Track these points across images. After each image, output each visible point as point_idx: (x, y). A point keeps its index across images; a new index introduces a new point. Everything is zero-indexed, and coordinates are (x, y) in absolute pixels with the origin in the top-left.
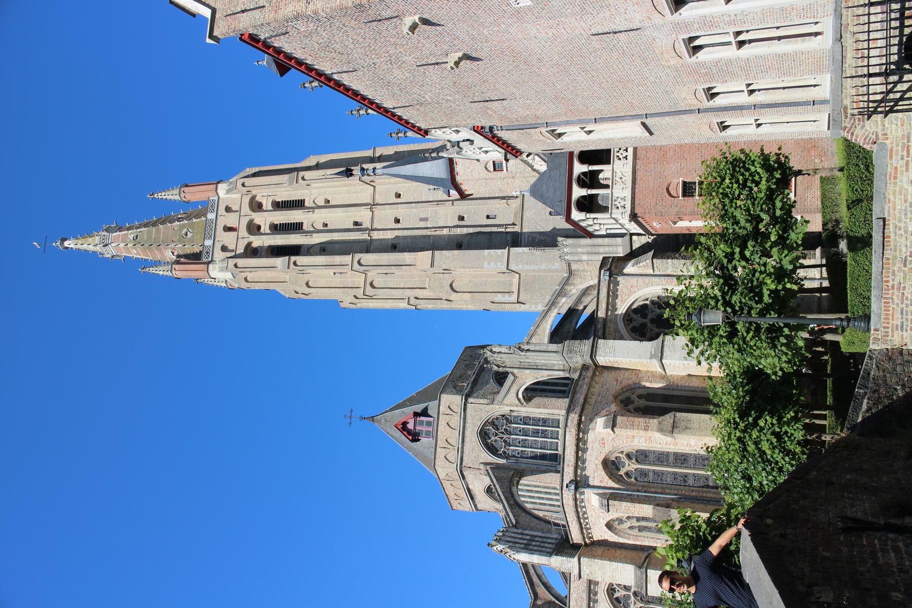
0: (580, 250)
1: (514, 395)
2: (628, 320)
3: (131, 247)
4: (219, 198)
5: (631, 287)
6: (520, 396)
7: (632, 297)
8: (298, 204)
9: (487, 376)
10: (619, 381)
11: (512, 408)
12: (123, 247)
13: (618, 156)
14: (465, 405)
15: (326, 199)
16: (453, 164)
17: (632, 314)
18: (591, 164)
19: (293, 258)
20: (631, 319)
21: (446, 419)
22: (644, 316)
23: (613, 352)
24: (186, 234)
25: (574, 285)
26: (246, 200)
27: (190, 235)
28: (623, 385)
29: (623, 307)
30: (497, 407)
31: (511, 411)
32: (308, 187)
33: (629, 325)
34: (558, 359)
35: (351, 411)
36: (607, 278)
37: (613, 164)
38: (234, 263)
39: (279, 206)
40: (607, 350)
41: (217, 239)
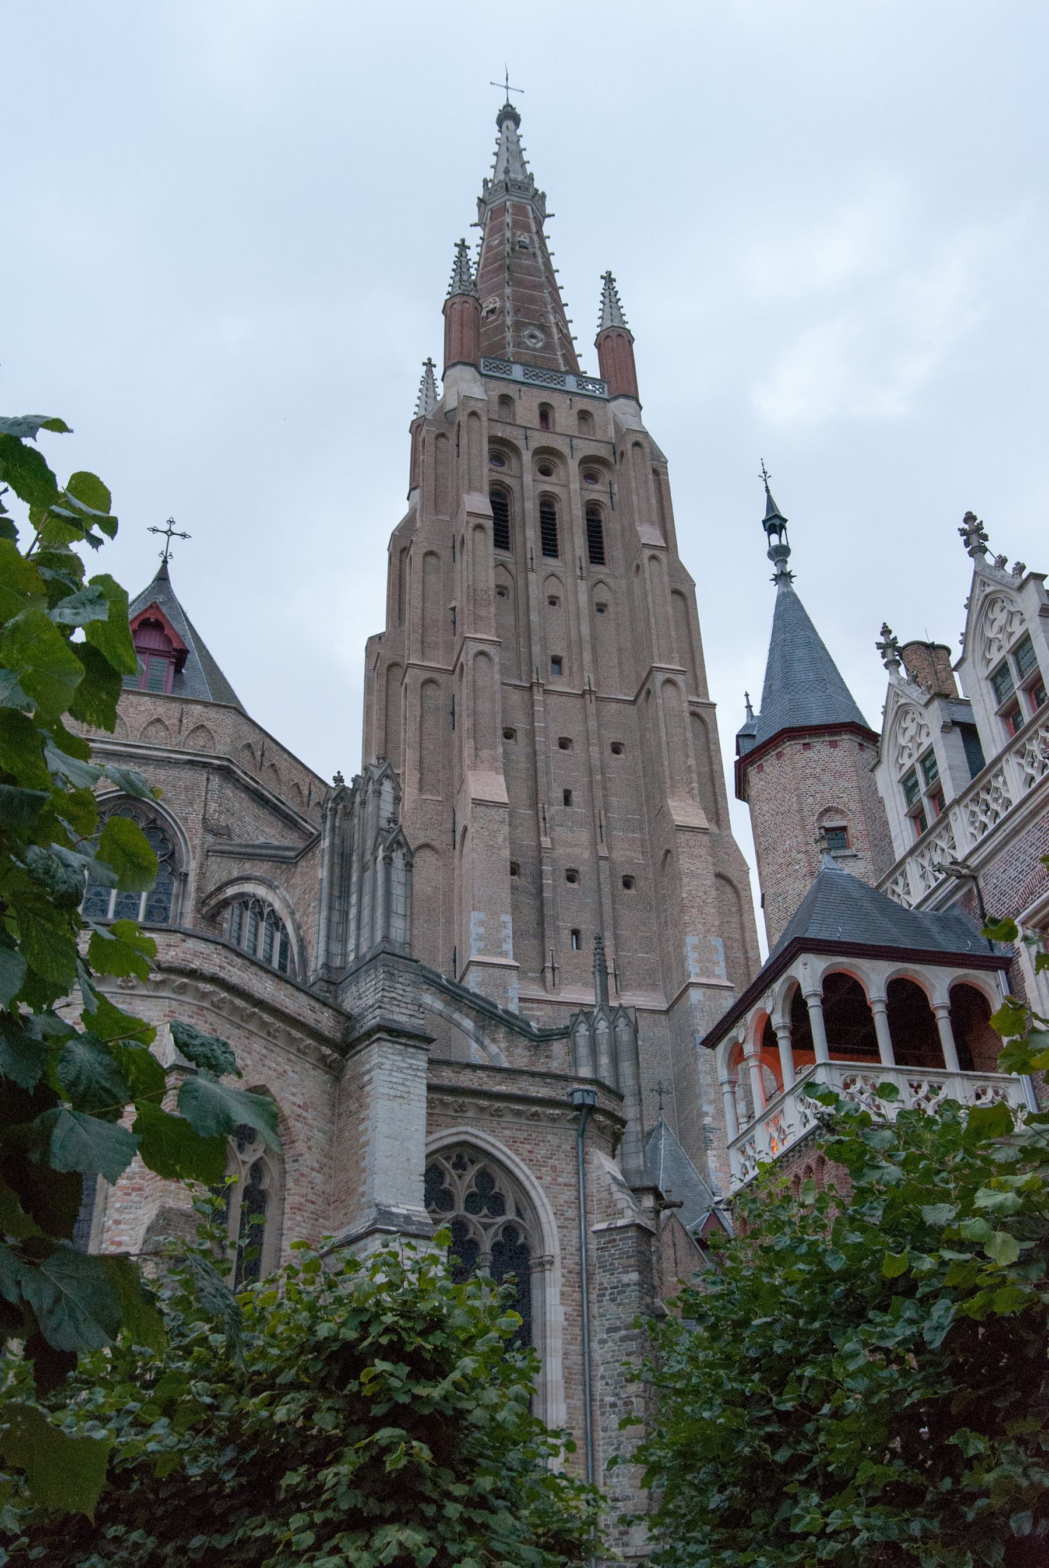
0: (604, 1060)
1: (235, 874)
2: (460, 1157)
3: (503, 235)
4: (608, 400)
5: (554, 1168)
6: (230, 891)
7: (522, 1164)
8: (596, 553)
9: (273, 832)
10: (304, 1114)
11: (192, 878)
12: (503, 221)
13: (984, 1092)
14: (205, 765)
15: (606, 605)
16: (831, 734)
17: (478, 1167)
18: (954, 1013)
19: (489, 524)
20: (464, 1169)
21: (169, 718)
22: (473, 1203)
23: (392, 1092)
24: (532, 336)
25: (508, 1049)
26: (603, 452)
27: (530, 343)
28: (291, 1122)
29: (499, 1144)
30: (197, 841)
31: (186, 875)
32: (634, 568)
33: (447, 1159)
34: (364, 949)
35: (184, 536)
36: (578, 1099)
37: (962, 1076)
39: (593, 515)
40: (398, 1077)
41: (524, 389)
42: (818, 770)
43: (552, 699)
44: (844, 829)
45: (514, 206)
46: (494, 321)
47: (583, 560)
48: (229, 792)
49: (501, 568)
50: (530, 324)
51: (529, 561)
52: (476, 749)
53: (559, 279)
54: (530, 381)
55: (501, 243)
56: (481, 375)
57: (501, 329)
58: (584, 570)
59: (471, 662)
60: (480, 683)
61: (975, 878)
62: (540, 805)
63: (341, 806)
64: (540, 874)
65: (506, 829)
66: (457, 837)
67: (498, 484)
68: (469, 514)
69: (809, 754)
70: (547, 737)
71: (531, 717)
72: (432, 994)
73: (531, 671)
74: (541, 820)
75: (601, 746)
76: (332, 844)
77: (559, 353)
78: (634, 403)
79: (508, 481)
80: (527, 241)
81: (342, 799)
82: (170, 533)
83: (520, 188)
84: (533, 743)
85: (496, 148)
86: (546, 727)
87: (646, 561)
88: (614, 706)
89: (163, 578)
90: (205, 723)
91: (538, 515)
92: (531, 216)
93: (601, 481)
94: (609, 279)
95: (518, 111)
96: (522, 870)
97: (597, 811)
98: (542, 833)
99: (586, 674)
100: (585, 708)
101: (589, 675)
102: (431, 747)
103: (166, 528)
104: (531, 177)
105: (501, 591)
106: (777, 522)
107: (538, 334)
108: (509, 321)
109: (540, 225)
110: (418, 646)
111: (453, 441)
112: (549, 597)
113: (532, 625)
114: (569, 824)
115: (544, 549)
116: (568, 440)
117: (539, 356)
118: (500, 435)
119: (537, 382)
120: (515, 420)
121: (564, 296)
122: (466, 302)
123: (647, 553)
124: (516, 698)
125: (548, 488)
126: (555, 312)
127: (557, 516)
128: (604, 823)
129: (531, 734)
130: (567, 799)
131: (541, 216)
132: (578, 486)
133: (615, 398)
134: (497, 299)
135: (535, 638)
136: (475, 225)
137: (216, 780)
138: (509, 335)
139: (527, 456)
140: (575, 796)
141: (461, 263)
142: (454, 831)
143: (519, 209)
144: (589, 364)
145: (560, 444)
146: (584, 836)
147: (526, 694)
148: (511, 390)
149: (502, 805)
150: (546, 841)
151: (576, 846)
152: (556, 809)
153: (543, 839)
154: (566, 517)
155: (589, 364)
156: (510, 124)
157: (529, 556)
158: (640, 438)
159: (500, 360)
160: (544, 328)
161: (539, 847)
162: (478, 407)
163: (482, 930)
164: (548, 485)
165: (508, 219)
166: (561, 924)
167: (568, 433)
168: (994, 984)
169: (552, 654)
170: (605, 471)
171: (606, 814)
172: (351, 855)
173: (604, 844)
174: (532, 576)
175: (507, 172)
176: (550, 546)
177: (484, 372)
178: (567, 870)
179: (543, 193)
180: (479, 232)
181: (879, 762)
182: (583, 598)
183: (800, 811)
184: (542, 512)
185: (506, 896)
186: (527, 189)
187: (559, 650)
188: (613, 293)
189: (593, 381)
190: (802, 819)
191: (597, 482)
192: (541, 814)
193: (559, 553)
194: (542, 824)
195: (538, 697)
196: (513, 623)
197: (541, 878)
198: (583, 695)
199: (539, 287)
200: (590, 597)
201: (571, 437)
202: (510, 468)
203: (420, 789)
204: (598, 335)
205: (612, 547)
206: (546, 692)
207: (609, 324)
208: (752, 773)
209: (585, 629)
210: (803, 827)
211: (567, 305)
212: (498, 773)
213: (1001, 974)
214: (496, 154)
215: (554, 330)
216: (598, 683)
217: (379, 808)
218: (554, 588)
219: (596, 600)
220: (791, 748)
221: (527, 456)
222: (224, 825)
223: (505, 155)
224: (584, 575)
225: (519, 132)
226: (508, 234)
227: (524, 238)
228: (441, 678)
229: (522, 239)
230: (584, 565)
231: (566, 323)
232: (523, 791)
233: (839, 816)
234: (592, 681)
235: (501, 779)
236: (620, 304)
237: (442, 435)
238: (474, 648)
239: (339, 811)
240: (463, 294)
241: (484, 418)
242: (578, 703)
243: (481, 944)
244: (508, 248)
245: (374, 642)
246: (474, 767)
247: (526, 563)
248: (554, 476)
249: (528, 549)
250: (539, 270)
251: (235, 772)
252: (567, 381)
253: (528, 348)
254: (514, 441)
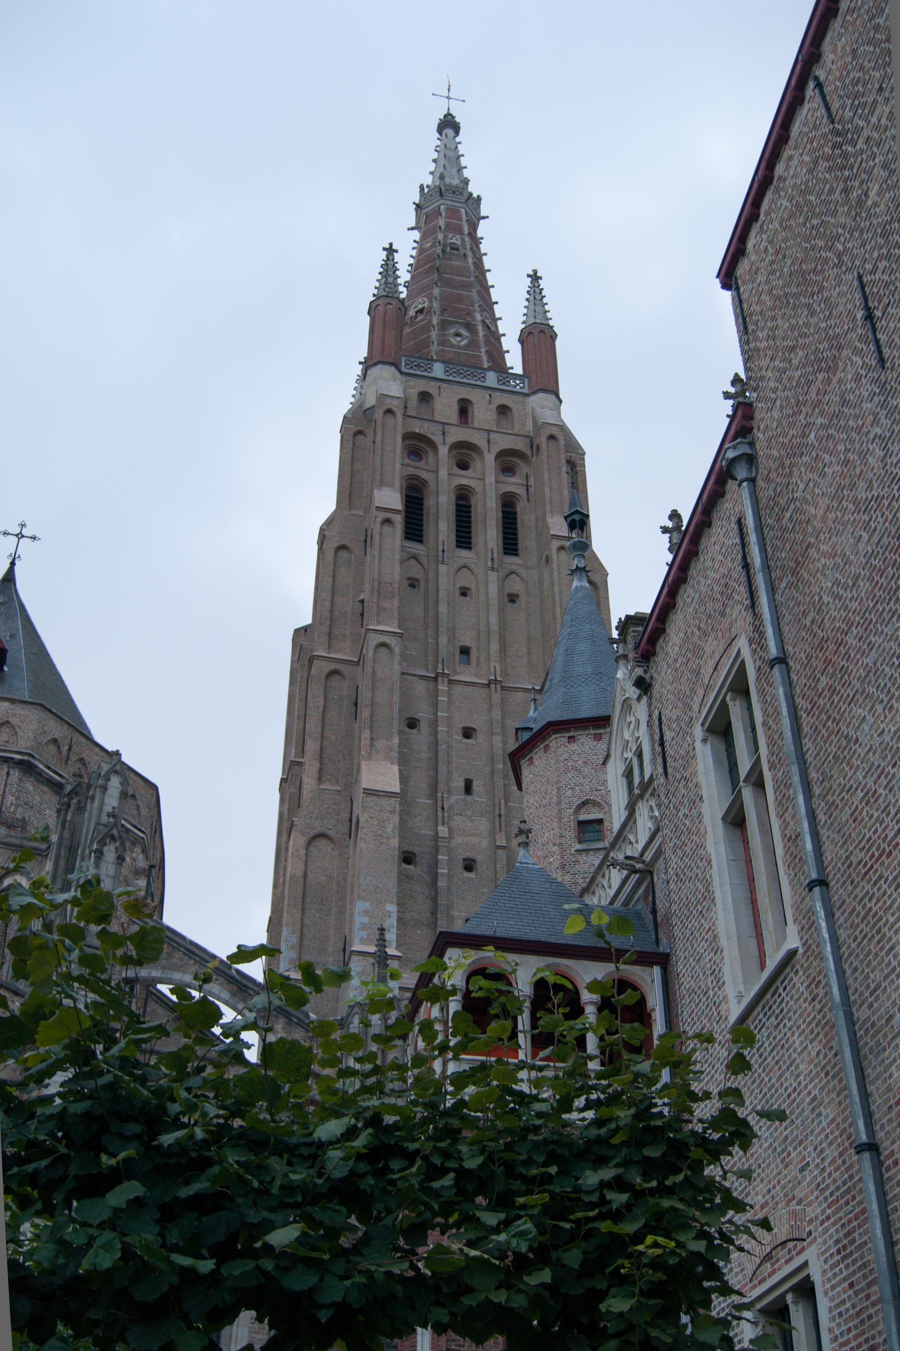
3: (436, 238)
4: (527, 395)
8: (510, 545)
15: (517, 596)
16: (595, 727)
19: (398, 519)
24: (458, 335)
26: (520, 445)
27: (454, 341)
32: (544, 559)
35: (34, 538)
38: (394, 409)
41: (444, 385)
42: (580, 763)
43: (458, 690)
44: (600, 821)
45: (448, 210)
46: (421, 321)
47: (495, 552)
48: (29, 786)
49: (413, 561)
51: (440, 553)
52: (372, 739)
53: (491, 278)
54: (451, 378)
55: (433, 246)
56: (402, 373)
57: (428, 327)
58: (496, 561)
59: (371, 654)
60: (379, 674)
61: (651, 873)
62: (439, 795)
63: (75, 801)
64: (435, 864)
65: (396, 819)
66: (352, 827)
67: (413, 479)
68: (378, 508)
69: (574, 747)
70: (450, 726)
71: (435, 705)
72: (221, 984)
73: (437, 662)
74: (439, 809)
75: (504, 735)
76: (61, 838)
77: (483, 350)
78: (553, 397)
79: (424, 475)
80: (459, 243)
81: (77, 794)
82: (20, 536)
83: (454, 192)
84: (435, 733)
85: (435, 155)
86: (449, 717)
87: (554, 551)
88: (520, 695)
90: (10, 720)
91: (453, 508)
92: (464, 218)
93: (518, 473)
94: (535, 277)
95: (457, 119)
96: (418, 859)
97: (497, 801)
98: (440, 822)
99: (492, 665)
100: (490, 697)
101: (495, 665)
102: (333, 737)
103: (17, 531)
104: (466, 182)
105: (413, 584)
106: (577, 517)
107: (463, 332)
108: (435, 320)
109: (474, 227)
110: (325, 638)
111: (370, 438)
112: (461, 588)
113: (440, 616)
114: (469, 813)
115: (457, 541)
116: (485, 435)
117: (462, 354)
118: (417, 431)
119: (458, 379)
120: (433, 416)
121: (495, 295)
122: (389, 303)
123: (556, 544)
124: (420, 688)
125: (464, 481)
126: (482, 310)
127: (472, 509)
128: (503, 812)
129: (434, 723)
130: (468, 788)
131: (475, 219)
132: (493, 479)
133: (534, 393)
134: (426, 299)
135: (442, 629)
136: (412, 229)
137: (16, 774)
138: (434, 334)
139: (443, 451)
140: (476, 786)
141: (389, 268)
142: (351, 821)
143: (453, 213)
144: (514, 361)
145: (478, 439)
146: (483, 825)
147: (431, 685)
148: (431, 388)
149: (392, 795)
150: (443, 830)
151: (474, 835)
152: (457, 798)
153: (440, 828)
154: (480, 510)
155: (514, 361)
156: (449, 132)
157: (441, 548)
158: (555, 431)
159: (421, 358)
160: (470, 327)
161: (436, 836)
162: (394, 405)
163: (365, 920)
164: (465, 479)
165: (441, 222)
166: (455, 913)
167: (485, 428)
168: (649, 981)
169: (462, 644)
170: (522, 464)
171: (506, 803)
172: (78, 849)
173: (503, 833)
174: (443, 568)
175: (442, 177)
176: (464, 539)
177: (404, 369)
178: (464, 860)
179: (479, 197)
180: (416, 235)
181: (608, 757)
182: (493, 589)
183: (559, 803)
184: (457, 505)
185: (392, 885)
186: (461, 193)
187: (467, 640)
188: (537, 291)
189: (515, 376)
190: (560, 812)
191: (514, 474)
192: (439, 804)
193: (473, 545)
194: (440, 814)
195: (443, 687)
196: (422, 614)
197: (437, 868)
198: (489, 685)
199: (467, 286)
200: (501, 587)
201: (489, 431)
202: (427, 463)
203: (320, 779)
204: (522, 331)
205: (526, 539)
206: (451, 682)
207: (532, 320)
208: (524, 764)
209: (494, 620)
210: (560, 820)
211: (497, 303)
212: (392, 763)
213: (657, 970)
214: (434, 161)
215: (480, 328)
216: (504, 672)
217: (102, 803)
218: (466, 579)
219: (508, 590)
220: (557, 741)
221: (443, 451)
222: (19, 816)
223: (442, 162)
224: (495, 566)
225: (458, 139)
226: (440, 237)
227: (456, 240)
228: (345, 669)
229: (454, 241)
230: (495, 556)
231: (495, 320)
232: (421, 781)
233: (596, 809)
234: (498, 669)
235: (395, 769)
236: (545, 300)
237: (360, 432)
238: (375, 640)
239: (72, 806)
240: (387, 296)
241: (399, 415)
242: (483, 692)
243: (364, 934)
244: (439, 250)
245: (301, 633)
246: (369, 757)
247: (437, 556)
248: (471, 470)
249: (440, 542)
250: (469, 271)
251: (37, 767)
252: (487, 377)
253: (452, 346)
254: (430, 436)
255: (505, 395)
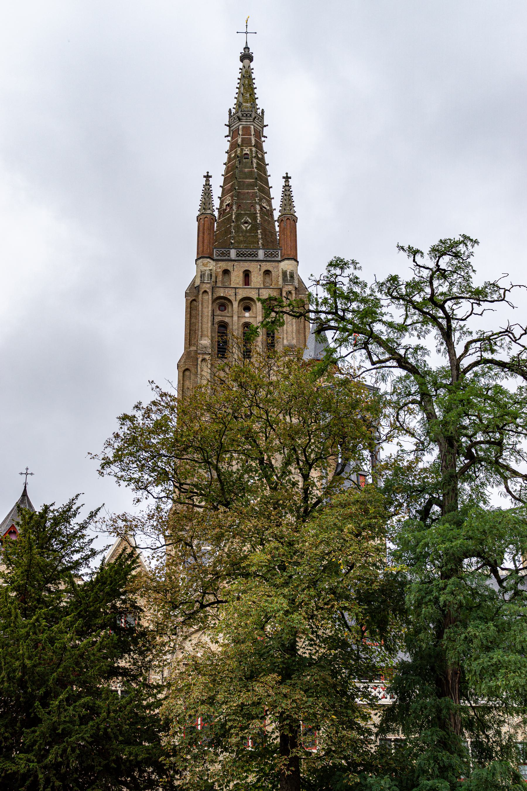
4: (280, 261)
35: (32, 474)
38: (208, 290)
50: (246, 214)
79: (227, 320)
82: (27, 474)
89: (25, 494)
92: (253, 133)
139: (235, 305)
156: (247, 61)
202: (228, 311)
221: (235, 305)
241: (210, 294)
255: (268, 264)
